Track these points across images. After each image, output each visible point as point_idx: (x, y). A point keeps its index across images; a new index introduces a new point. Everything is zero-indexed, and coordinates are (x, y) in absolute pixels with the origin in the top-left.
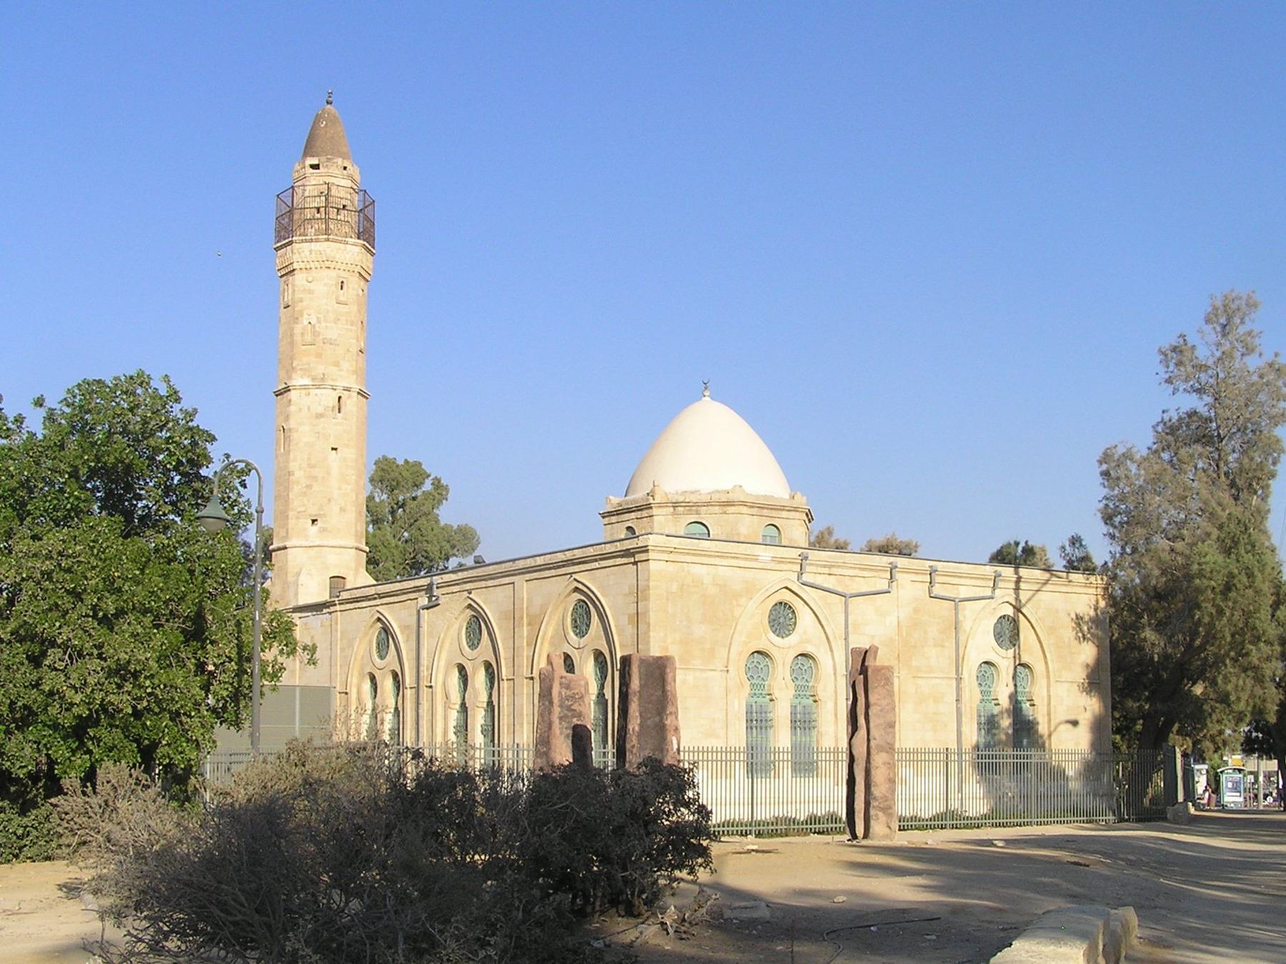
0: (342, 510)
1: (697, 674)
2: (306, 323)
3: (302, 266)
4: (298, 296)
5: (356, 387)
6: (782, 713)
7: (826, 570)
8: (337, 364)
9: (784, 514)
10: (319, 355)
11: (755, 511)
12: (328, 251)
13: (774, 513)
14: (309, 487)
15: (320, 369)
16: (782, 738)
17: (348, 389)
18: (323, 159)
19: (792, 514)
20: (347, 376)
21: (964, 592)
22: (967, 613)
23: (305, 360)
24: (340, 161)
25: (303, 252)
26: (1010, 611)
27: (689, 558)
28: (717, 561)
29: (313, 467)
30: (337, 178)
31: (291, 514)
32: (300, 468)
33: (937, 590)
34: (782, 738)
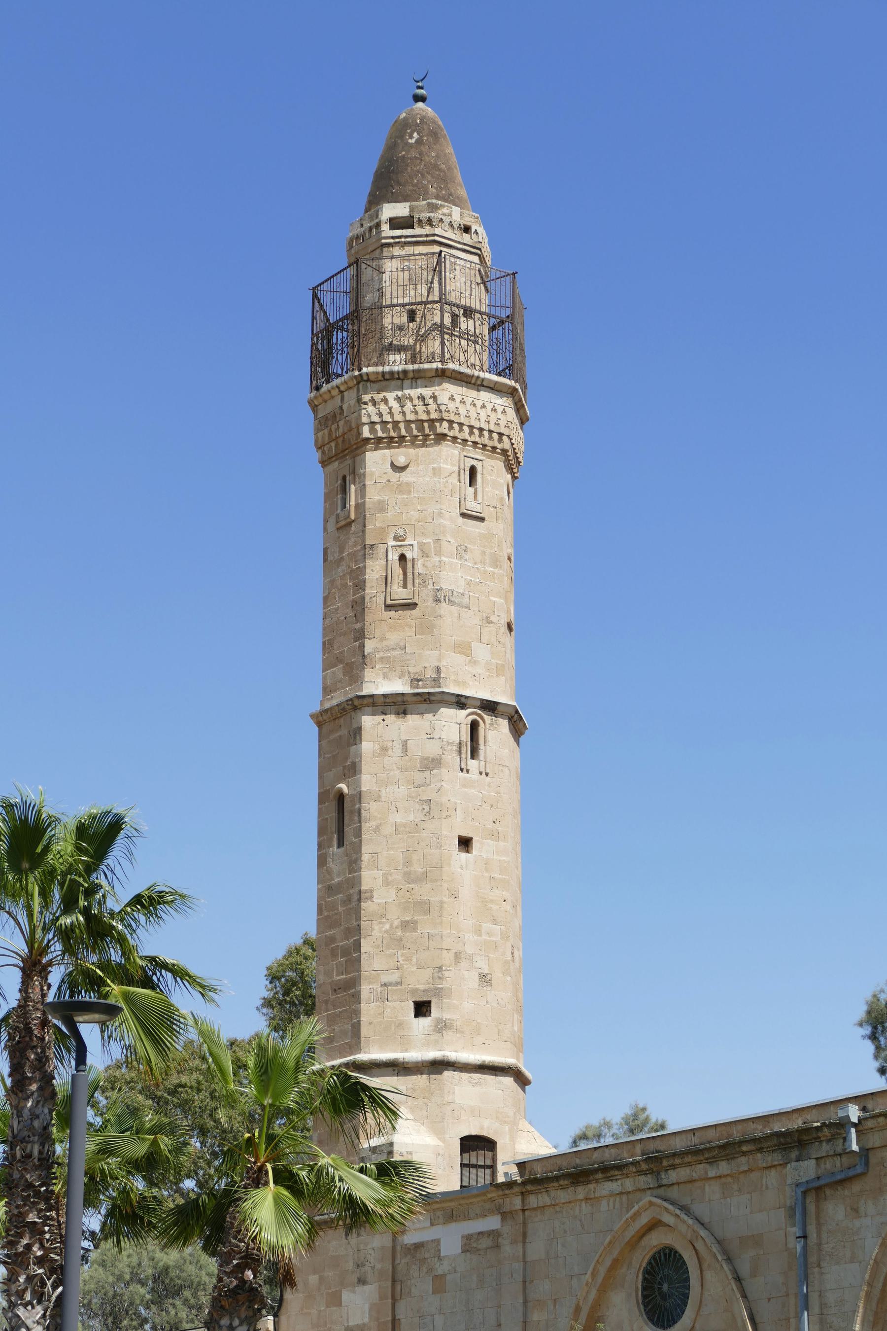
0: (485, 979)
2: (394, 556)
4: (372, 496)
8: (464, 649)
12: (443, 398)
23: (393, 638)
29: (411, 878)
31: (365, 989)
32: (387, 883)
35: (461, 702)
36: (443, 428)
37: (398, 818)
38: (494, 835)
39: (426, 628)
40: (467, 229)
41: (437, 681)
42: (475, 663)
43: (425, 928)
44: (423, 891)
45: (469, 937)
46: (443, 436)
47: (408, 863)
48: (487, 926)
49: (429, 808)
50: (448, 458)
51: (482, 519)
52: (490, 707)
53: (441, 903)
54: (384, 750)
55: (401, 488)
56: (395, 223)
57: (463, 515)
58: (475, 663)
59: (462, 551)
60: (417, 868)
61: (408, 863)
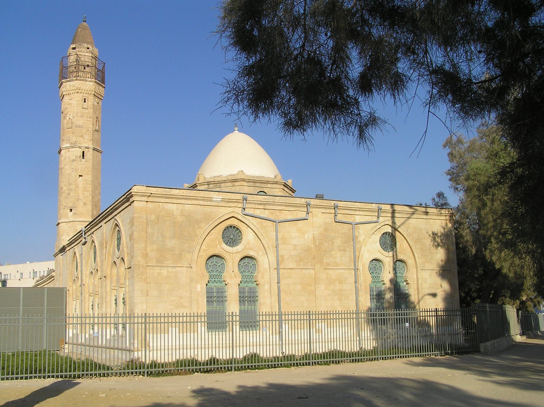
0: (85, 204)
1: (170, 269)
2: (68, 118)
3: (67, 93)
5: (91, 146)
6: (232, 293)
7: (262, 207)
8: (82, 136)
9: (269, 186)
10: (73, 133)
11: (251, 184)
13: (263, 185)
14: (69, 194)
15: (74, 139)
16: (233, 307)
17: (87, 148)
18: (77, 44)
19: (275, 186)
20: (87, 142)
21: (358, 219)
22: (361, 231)
23: (68, 135)
24: (85, 45)
25: (68, 86)
26: (389, 230)
27: (163, 200)
28: (183, 201)
30: (84, 53)
32: (65, 186)
33: (340, 217)
34: (233, 307)
37: (67, 172)
38: (88, 174)
45: (81, 195)
48: (86, 193)
56: (74, 48)
60: (71, 182)
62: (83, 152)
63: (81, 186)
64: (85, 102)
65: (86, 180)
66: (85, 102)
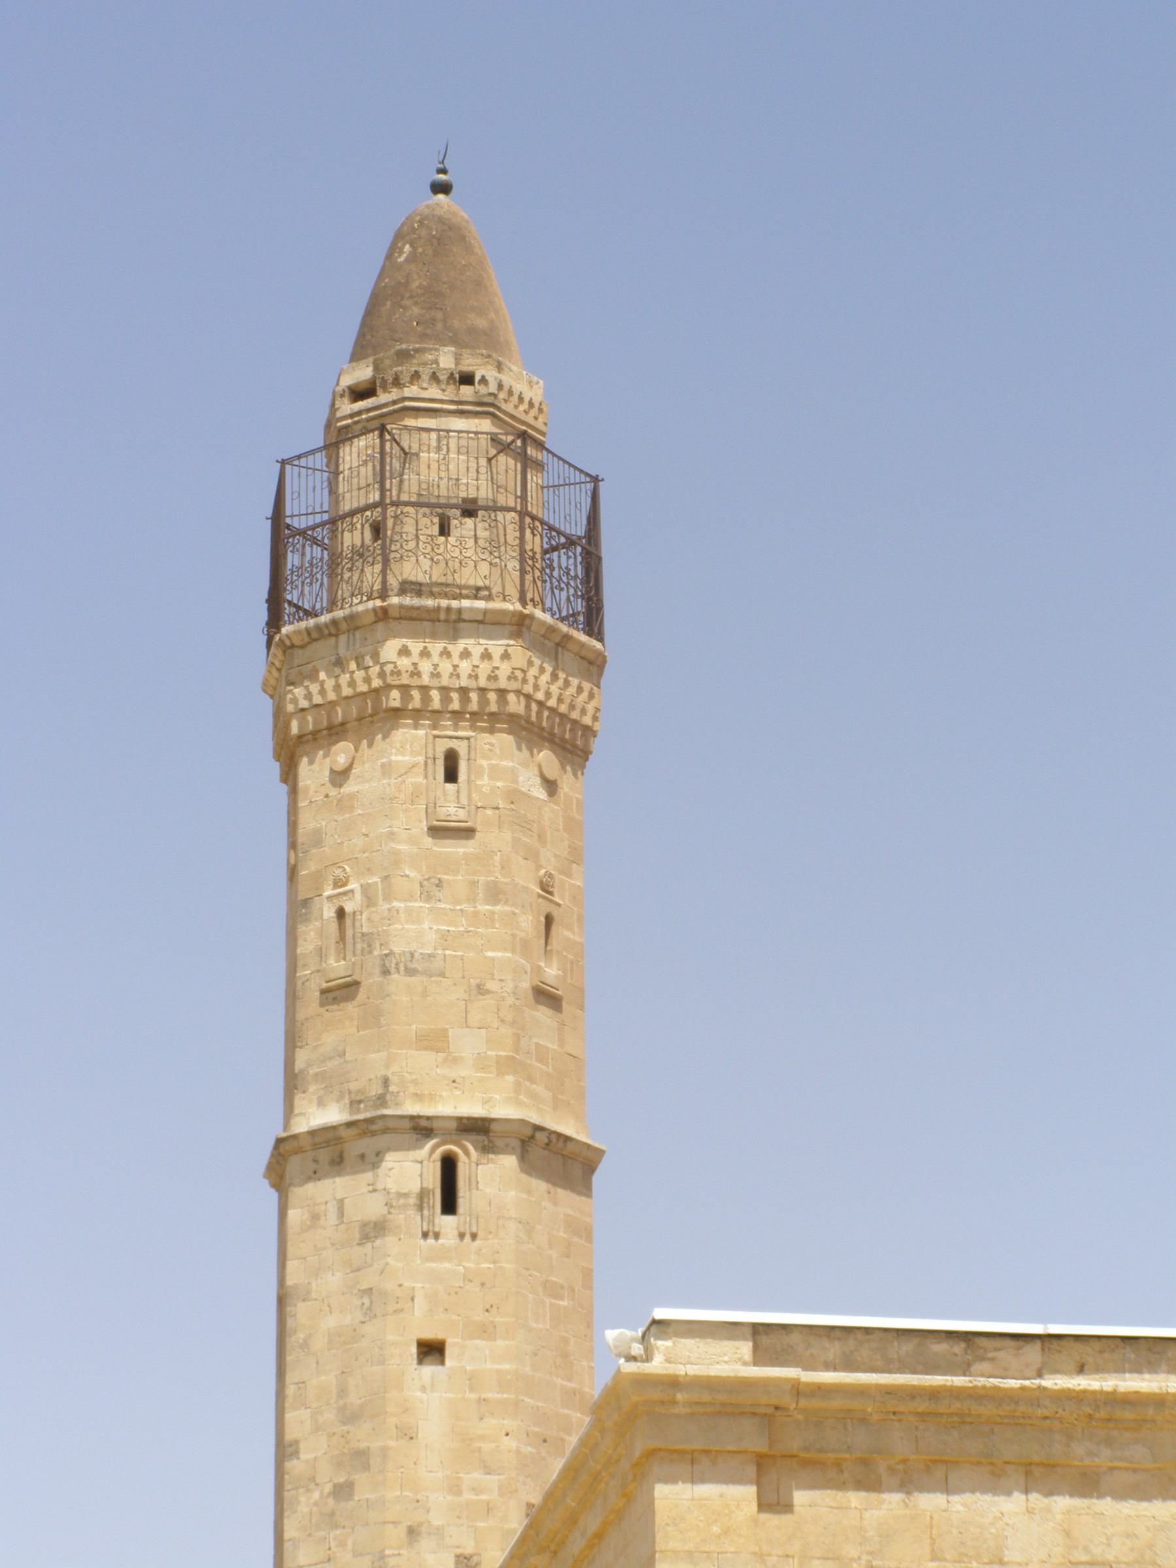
2: (329, 912)
8: (434, 1041)
14: (343, 1491)
23: (330, 1040)
35: (422, 1128)
36: (394, 699)
37: (330, 1322)
38: (485, 1331)
39: (372, 1018)
40: (467, 379)
41: (381, 1100)
42: (455, 1061)
43: (363, 1492)
44: (361, 1435)
46: (396, 713)
47: (343, 1392)
49: (372, 1301)
50: (408, 748)
51: (468, 833)
52: (477, 1129)
53: (384, 1450)
54: (315, 1217)
55: (345, 804)
57: (437, 832)
58: (455, 1061)
59: (432, 887)
60: (354, 1399)
61: (343, 1392)
62: (449, 1166)
63: (433, 1427)
64: (451, 776)
65: (473, 1380)
66: (451, 776)
